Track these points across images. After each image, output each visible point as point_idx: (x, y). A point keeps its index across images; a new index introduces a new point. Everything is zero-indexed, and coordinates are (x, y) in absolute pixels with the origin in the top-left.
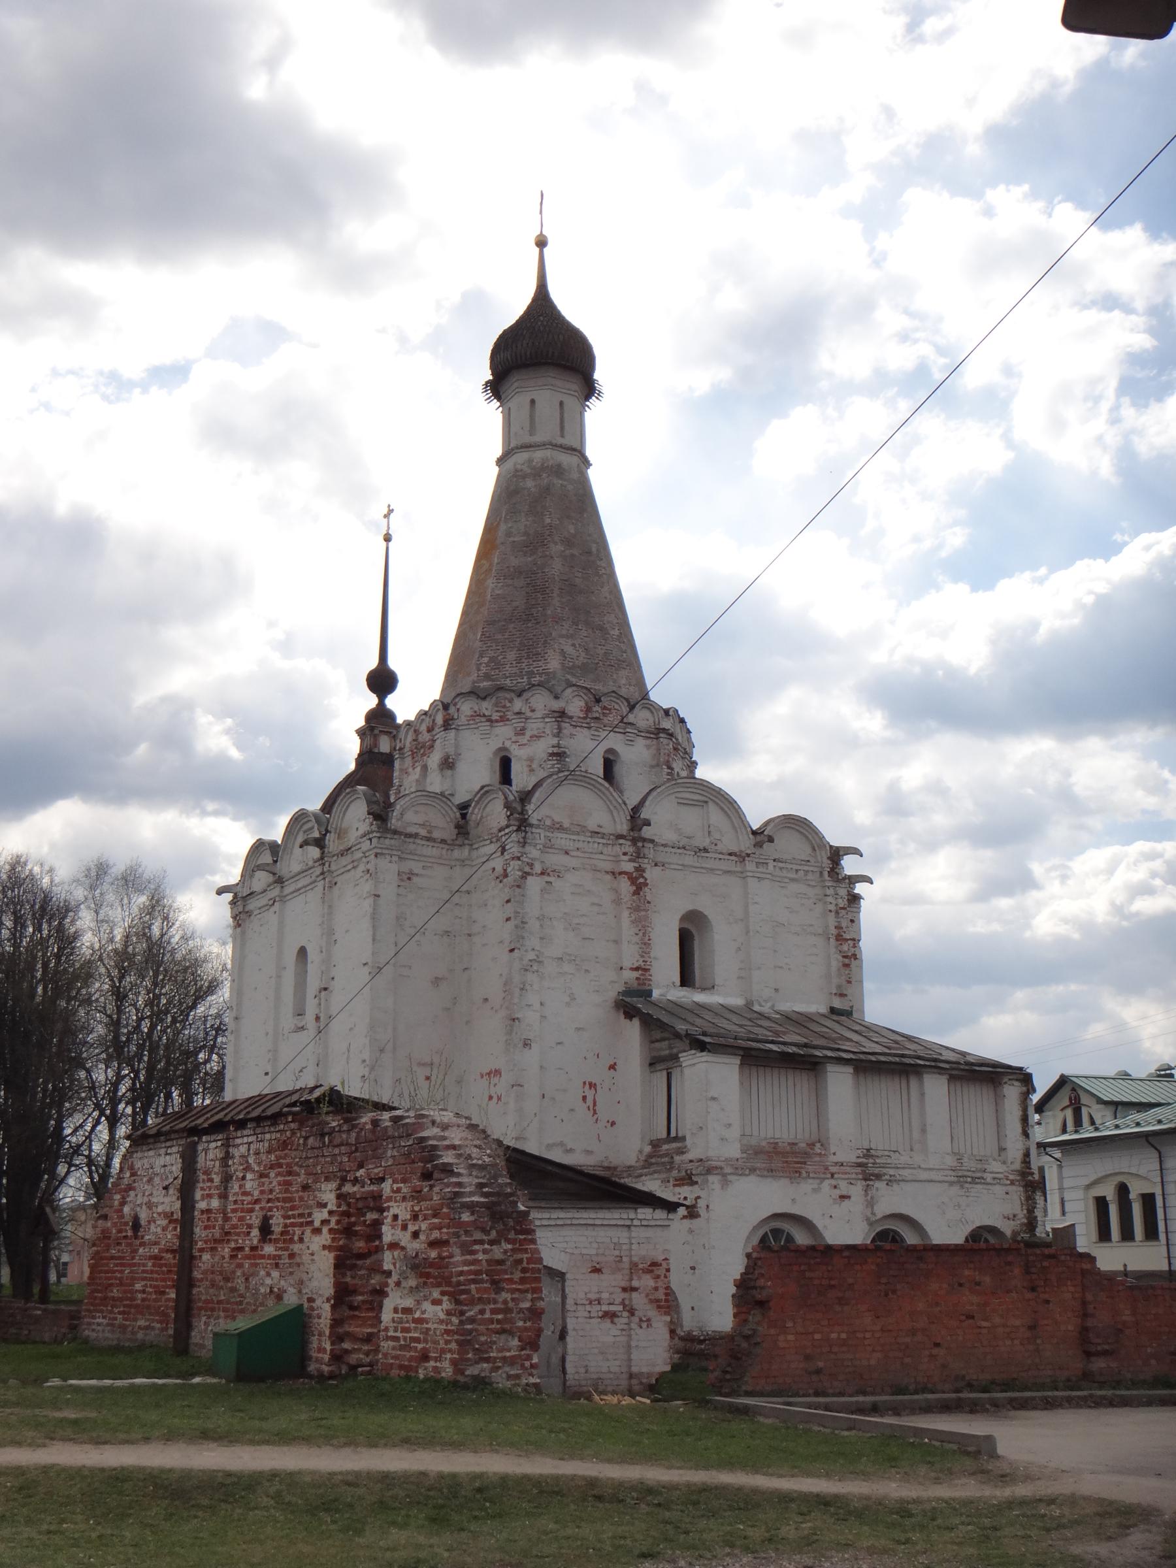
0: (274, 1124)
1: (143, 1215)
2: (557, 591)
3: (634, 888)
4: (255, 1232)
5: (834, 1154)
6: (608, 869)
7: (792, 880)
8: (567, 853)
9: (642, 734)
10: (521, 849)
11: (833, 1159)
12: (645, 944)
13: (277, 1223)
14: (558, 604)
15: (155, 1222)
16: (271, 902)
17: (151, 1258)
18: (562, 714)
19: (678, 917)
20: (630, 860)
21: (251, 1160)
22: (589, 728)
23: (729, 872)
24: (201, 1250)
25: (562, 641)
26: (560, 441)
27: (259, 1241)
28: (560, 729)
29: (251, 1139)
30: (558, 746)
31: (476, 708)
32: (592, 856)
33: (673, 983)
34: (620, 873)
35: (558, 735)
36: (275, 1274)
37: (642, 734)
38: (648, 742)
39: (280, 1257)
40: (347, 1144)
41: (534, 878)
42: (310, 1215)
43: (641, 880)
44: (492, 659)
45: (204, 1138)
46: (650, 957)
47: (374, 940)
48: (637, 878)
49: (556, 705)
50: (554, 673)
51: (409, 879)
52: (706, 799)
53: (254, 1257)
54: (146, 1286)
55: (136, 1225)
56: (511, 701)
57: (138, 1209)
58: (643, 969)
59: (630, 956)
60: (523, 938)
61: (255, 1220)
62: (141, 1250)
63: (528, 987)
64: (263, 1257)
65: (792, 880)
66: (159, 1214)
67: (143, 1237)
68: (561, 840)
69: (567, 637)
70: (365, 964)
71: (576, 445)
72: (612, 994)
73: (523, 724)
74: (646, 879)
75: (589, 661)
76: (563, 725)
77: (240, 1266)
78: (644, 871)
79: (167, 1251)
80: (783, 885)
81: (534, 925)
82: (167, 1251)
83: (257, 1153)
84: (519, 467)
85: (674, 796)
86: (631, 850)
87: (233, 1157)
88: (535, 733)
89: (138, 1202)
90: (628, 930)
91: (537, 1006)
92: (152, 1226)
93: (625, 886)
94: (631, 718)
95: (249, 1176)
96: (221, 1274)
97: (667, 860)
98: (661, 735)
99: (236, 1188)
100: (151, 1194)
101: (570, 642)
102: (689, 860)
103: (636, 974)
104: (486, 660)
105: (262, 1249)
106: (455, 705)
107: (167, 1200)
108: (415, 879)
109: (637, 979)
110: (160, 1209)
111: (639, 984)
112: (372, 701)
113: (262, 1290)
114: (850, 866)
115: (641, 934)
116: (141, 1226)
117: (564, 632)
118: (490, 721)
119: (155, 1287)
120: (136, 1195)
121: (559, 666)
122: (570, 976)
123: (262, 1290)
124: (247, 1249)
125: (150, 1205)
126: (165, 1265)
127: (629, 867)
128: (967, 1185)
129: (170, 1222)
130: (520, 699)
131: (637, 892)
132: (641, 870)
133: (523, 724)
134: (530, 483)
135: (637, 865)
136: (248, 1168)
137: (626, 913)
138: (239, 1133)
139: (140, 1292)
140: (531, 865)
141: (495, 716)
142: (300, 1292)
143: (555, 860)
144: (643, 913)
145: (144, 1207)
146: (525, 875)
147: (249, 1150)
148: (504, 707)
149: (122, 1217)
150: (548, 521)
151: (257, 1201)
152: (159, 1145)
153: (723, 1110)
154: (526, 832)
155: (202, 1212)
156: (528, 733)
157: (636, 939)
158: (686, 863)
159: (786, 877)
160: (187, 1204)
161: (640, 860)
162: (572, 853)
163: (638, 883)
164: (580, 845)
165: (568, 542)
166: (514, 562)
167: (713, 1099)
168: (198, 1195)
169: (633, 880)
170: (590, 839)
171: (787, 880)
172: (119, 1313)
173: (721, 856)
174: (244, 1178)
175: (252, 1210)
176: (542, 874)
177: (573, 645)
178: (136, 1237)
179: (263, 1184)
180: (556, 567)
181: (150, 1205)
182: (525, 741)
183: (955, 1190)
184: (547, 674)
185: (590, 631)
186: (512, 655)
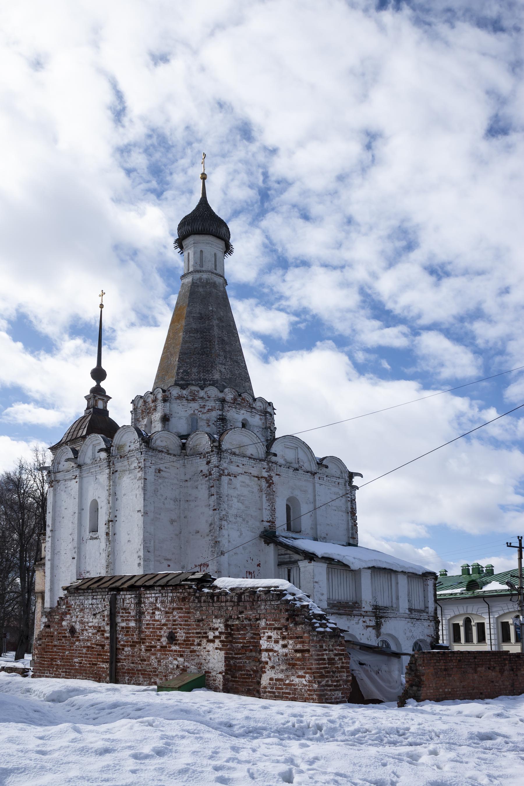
0: (176, 589)
1: (78, 627)
2: (216, 342)
4: (164, 641)
6: (256, 475)
8: (238, 466)
10: (219, 463)
13: (181, 635)
14: (217, 348)
15: (87, 630)
16: (74, 477)
17: (84, 647)
18: (223, 401)
19: (286, 499)
20: (266, 471)
21: (159, 605)
22: (236, 408)
24: (124, 646)
25: (220, 366)
26: (215, 271)
27: (168, 643)
28: (223, 407)
29: (157, 595)
30: (222, 415)
31: (180, 393)
34: (262, 477)
35: (222, 410)
36: (181, 659)
39: (184, 652)
40: (231, 601)
42: (206, 633)
43: (271, 481)
44: (185, 371)
45: (121, 593)
47: (144, 500)
49: (221, 395)
50: (217, 380)
51: (159, 472)
52: (297, 446)
53: (165, 651)
54: (82, 660)
55: (73, 630)
56: (198, 392)
57: (74, 624)
59: (266, 517)
61: (164, 632)
62: (77, 643)
64: (172, 651)
66: (90, 627)
67: (78, 637)
68: (234, 458)
69: (222, 364)
70: (138, 511)
71: (222, 274)
72: (258, 532)
73: (204, 403)
77: (154, 654)
78: (272, 477)
79: (97, 645)
82: (97, 645)
83: (162, 602)
84: (195, 281)
86: (267, 467)
87: (144, 603)
88: (210, 408)
89: (73, 620)
90: (266, 505)
91: (226, 536)
92: (85, 632)
93: (264, 484)
94: (254, 406)
95: (157, 613)
96: (139, 657)
99: (148, 618)
100: (83, 617)
101: (224, 367)
104: (181, 371)
105: (170, 647)
106: (169, 391)
107: (95, 621)
108: (162, 473)
110: (90, 624)
112: (94, 384)
113: (171, 666)
114: (356, 481)
116: (76, 631)
117: (221, 362)
118: (187, 400)
119: (89, 661)
120: (72, 617)
121: (219, 378)
123: (171, 666)
124: (158, 647)
125: (82, 622)
126: (97, 651)
127: (265, 474)
129: (98, 631)
130: (203, 391)
131: (269, 487)
133: (204, 403)
134: (201, 290)
135: (269, 474)
136: (158, 609)
137: (264, 496)
138: (148, 592)
139: (77, 663)
140: (223, 470)
141: (190, 398)
142: (200, 668)
143: (233, 469)
144: (272, 496)
145: (78, 623)
146: (220, 475)
147: (156, 600)
148: (194, 394)
149: (62, 626)
150: (211, 308)
151: (164, 625)
152: (87, 594)
155: (123, 628)
156: (207, 408)
160: (113, 624)
165: (220, 319)
166: (194, 326)
167: (316, 582)
168: (119, 620)
169: (267, 481)
172: (63, 672)
174: (154, 613)
175: (161, 629)
176: (228, 475)
177: (225, 368)
178: (73, 637)
179: (169, 617)
180: (216, 331)
181: (82, 622)
182: (205, 411)
184: (213, 381)
185: (232, 363)
186: (195, 370)
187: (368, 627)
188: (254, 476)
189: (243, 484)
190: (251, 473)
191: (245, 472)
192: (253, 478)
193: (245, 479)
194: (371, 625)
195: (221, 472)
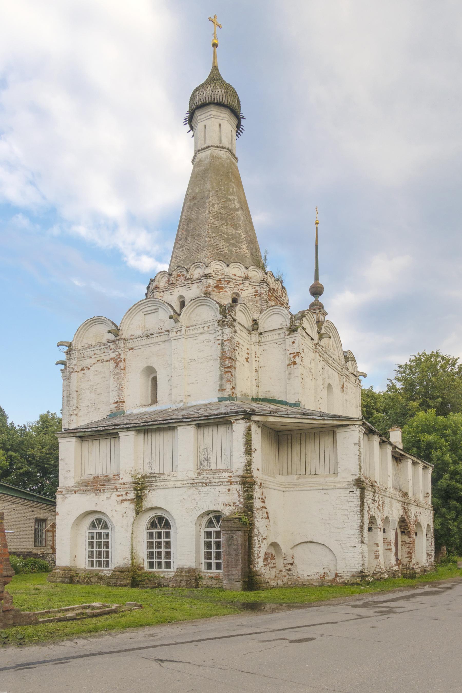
3: (116, 364)
5: (122, 479)
7: (201, 334)
8: (91, 357)
9: (195, 282)
11: (121, 481)
12: (120, 390)
23: (166, 341)
32: (101, 355)
33: (137, 405)
37: (195, 282)
38: (199, 284)
41: (74, 373)
43: (119, 360)
46: (122, 396)
48: (117, 359)
58: (120, 402)
59: (114, 398)
60: (70, 401)
63: (72, 422)
65: (201, 334)
74: (121, 359)
75: (188, 255)
76: (154, 293)
80: (196, 338)
81: (74, 394)
85: (141, 312)
90: (113, 385)
93: (112, 365)
97: (134, 346)
98: (202, 278)
102: (145, 341)
103: (116, 405)
109: (116, 407)
111: (117, 410)
115: (118, 386)
122: (92, 413)
127: (113, 355)
128: (200, 488)
131: (117, 366)
132: (119, 355)
135: (117, 353)
137: (112, 377)
153: (66, 464)
154: (71, 354)
157: (116, 388)
158: (142, 344)
159: (196, 334)
161: (118, 350)
162: (92, 357)
163: (117, 362)
164: (96, 352)
170: (99, 348)
171: (198, 335)
173: (160, 334)
183: (193, 490)
187: (123, 501)
188: (107, 361)
189: (96, 373)
190: (103, 360)
191: (98, 361)
192: (105, 363)
193: (99, 367)
194: (128, 498)
195: (72, 370)
